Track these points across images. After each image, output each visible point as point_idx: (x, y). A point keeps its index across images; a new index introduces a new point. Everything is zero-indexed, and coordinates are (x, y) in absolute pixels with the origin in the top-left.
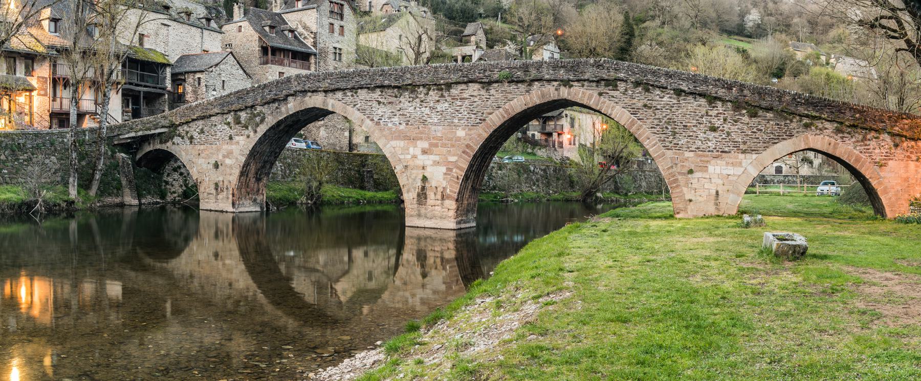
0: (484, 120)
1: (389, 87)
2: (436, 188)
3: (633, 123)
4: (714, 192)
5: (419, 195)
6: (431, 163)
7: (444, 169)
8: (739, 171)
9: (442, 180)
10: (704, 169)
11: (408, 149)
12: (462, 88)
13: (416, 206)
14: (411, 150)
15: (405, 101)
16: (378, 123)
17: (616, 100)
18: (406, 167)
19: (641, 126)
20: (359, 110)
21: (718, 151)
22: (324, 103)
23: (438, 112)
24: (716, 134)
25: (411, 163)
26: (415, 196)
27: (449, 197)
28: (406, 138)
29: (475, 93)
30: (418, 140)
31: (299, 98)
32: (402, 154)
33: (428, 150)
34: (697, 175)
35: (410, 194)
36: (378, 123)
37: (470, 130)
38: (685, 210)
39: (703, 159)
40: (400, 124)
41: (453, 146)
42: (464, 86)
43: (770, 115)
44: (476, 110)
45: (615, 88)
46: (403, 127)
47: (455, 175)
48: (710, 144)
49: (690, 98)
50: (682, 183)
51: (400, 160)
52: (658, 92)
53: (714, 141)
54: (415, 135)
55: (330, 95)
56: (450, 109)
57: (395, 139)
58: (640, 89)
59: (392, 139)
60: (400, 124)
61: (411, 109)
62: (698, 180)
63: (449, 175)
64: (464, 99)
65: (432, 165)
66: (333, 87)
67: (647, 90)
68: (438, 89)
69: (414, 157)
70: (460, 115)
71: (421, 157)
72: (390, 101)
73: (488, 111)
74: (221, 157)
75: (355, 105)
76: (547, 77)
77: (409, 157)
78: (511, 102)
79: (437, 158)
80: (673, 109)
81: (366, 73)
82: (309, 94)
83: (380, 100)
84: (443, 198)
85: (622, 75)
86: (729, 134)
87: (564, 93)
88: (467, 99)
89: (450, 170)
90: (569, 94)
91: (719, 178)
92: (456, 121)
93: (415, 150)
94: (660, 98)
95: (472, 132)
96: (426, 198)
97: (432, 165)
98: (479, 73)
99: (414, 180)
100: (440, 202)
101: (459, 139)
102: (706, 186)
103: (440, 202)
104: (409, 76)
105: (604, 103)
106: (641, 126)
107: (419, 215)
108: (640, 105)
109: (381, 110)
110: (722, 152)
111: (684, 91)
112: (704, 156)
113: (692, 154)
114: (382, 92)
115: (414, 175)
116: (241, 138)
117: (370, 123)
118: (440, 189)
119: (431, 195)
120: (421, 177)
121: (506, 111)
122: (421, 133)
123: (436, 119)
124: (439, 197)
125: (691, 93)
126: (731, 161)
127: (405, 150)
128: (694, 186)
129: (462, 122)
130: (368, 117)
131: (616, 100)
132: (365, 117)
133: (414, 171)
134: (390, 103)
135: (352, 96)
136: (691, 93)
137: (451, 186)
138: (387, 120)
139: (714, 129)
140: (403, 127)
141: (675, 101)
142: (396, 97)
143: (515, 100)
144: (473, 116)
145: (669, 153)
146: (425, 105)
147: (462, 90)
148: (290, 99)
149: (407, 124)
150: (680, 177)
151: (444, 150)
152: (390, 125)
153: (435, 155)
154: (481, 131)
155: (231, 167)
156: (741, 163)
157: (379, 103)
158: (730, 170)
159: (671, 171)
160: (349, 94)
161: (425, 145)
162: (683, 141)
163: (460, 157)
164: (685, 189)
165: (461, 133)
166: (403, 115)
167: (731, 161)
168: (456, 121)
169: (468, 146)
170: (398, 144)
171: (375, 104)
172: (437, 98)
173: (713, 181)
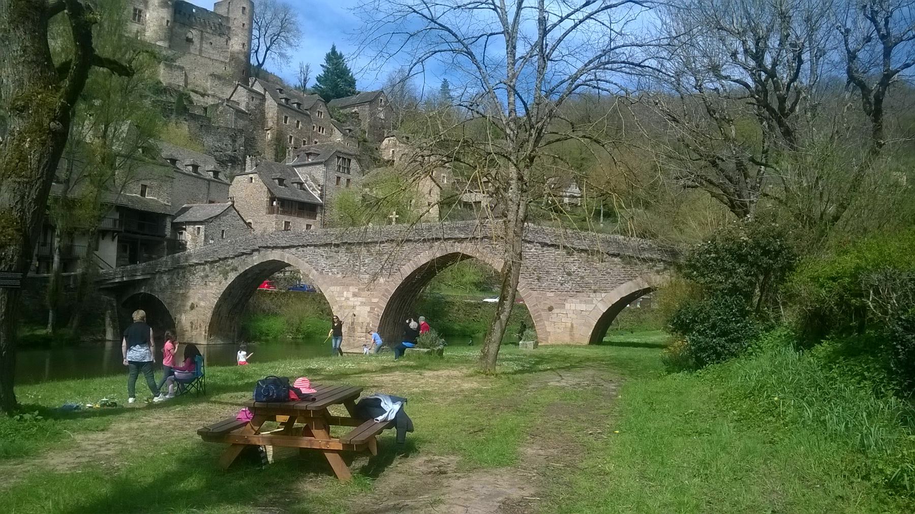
1: (330, 244)
7: (368, 309)
8: (590, 307)
10: (562, 306)
14: (345, 293)
16: (321, 273)
21: (573, 291)
25: (345, 304)
36: (321, 273)
38: (547, 339)
39: (561, 298)
40: (338, 273)
43: (616, 260)
46: (339, 276)
47: (376, 313)
53: (570, 284)
57: (333, 286)
60: (338, 273)
62: (557, 315)
63: (372, 313)
69: (347, 299)
71: (352, 299)
77: (343, 299)
79: (364, 300)
81: (314, 233)
91: (573, 313)
94: (529, 249)
102: (563, 320)
107: (349, 345)
113: (552, 294)
117: (316, 272)
121: (415, 263)
124: (364, 330)
125: (552, 245)
126: (584, 299)
127: (341, 294)
130: (314, 268)
132: (312, 267)
133: (347, 310)
152: (330, 274)
153: (363, 297)
158: (583, 307)
159: (535, 308)
163: (381, 299)
169: (387, 290)
173: (569, 316)
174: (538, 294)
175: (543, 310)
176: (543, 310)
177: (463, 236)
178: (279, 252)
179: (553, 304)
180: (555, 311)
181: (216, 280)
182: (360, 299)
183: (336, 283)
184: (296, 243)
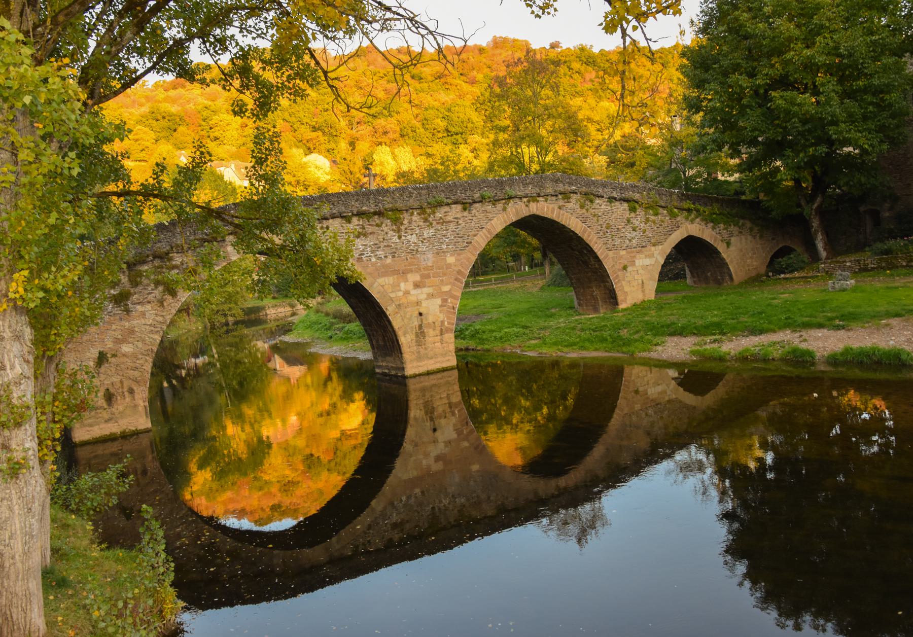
0: (471, 243)
2: (434, 323)
3: (585, 231)
4: (640, 282)
5: (417, 335)
6: (425, 296)
7: (438, 301)
9: (438, 314)
11: (399, 286)
12: (445, 210)
13: (415, 348)
14: (402, 285)
18: (399, 305)
19: (590, 233)
23: (424, 239)
25: (404, 301)
26: (413, 337)
28: (395, 272)
29: (458, 216)
30: (408, 273)
32: (392, 292)
33: (420, 282)
35: (408, 335)
37: (459, 255)
38: (625, 301)
40: (386, 257)
41: (445, 274)
44: (462, 233)
46: (389, 261)
47: (451, 305)
49: (617, 203)
51: (391, 299)
54: (404, 268)
59: (379, 276)
60: (386, 257)
63: (445, 306)
65: (426, 299)
69: (407, 293)
71: (413, 292)
73: (473, 233)
74: (110, 345)
77: (401, 294)
78: (492, 222)
84: (442, 333)
88: (451, 222)
89: (444, 301)
90: (537, 209)
92: (444, 247)
97: (426, 299)
98: (461, 193)
99: (410, 319)
100: (439, 337)
101: (449, 266)
103: (439, 337)
105: (563, 215)
106: (590, 233)
107: (419, 358)
110: (643, 247)
112: (632, 252)
115: (409, 314)
116: (149, 307)
118: (438, 324)
120: (417, 313)
121: (489, 231)
122: (410, 264)
123: (424, 247)
124: (438, 332)
127: (396, 287)
129: (450, 247)
136: (620, 200)
138: (370, 254)
140: (389, 261)
141: (609, 208)
143: (495, 219)
145: (611, 253)
146: (410, 232)
147: (446, 212)
149: (394, 257)
151: (437, 280)
152: (373, 260)
153: (429, 287)
154: (469, 255)
155: (134, 356)
156: (653, 254)
163: (453, 285)
164: (623, 282)
165: (451, 260)
166: (388, 246)
167: (647, 253)
168: (444, 247)
169: (459, 272)
170: (387, 281)
173: (639, 272)
174: (614, 253)
175: (619, 270)
176: (619, 270)
180: (629, 269)
181: (150, 297)
182: (426, 290)
183: (387, 271)
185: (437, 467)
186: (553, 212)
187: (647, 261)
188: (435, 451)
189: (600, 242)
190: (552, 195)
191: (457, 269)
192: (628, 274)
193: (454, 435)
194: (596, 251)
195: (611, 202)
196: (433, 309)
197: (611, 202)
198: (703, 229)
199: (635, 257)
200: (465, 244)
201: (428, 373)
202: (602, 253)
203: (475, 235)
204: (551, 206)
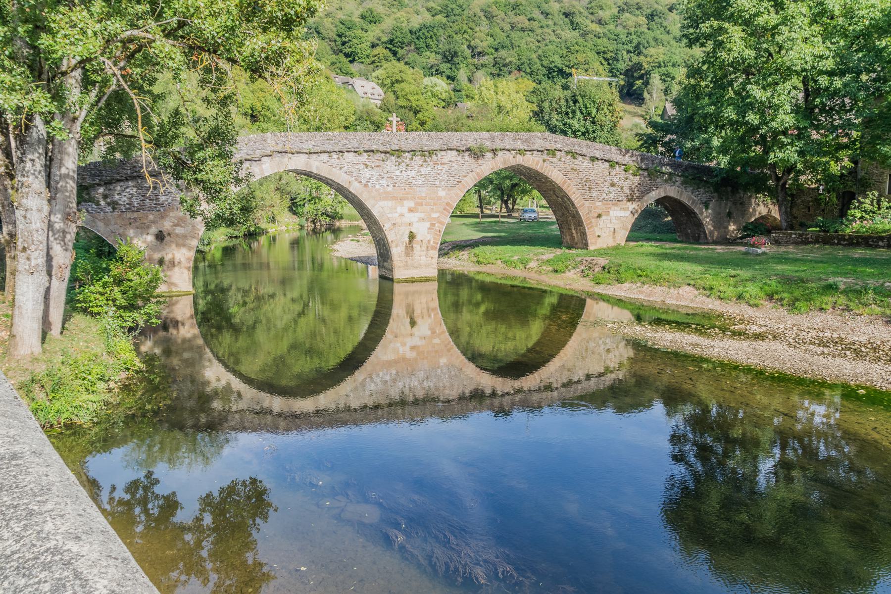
3: (565, 182)
5: (406, 247)
6: (417, 219)
7: (428, 225)
13: (404, 258)
14: (399, 209)
15: (390, 164)
16: (366, 186)
17: (555, 165)
20: (346, 173)
22: (307, 164)
24: (614, 189)
26: (403, 249)
27: (433, 248)
28: (394, 198)
31: (277, 158)
34: (603, 218)
35: (399, 248)
38: (595, 243)
41: (435, 204)
42: (443, 153)
43: (646, 173)
45: (554, 155)
48: (611, 195)
50: (594, 224)
52: (580, 158)
55: (315, 156)
56: (432, 173)
58: (569, 156)
61: (398, 173)
64: (444, 164)
66: (318, 149)
67: (575, 158)
68: (422, 155)
69: (402, 215)
70: (441, 178)
72: (377, 164)
73: (464, 174)
75: (341, 168)
76: (508, 147)
77: (397, 215)
79: (422, 215)
80: (590, 171)
82: (290, 155)
83: (367, 163)
85: (559, 146)
86: (622, 188)
87: (520, 160)
90: (523, 161)
92: (437, 183)
93: (403, 209)
95: (452, 192)
96: (412, 250)
99: (402, 235)
101: (440, 198)
104: (396, 142)
105: (546, 167)
107: (406, 266)
108: (569, 168)
109: (367, 173)
111: (597, 159)
112: (607, 204)
114: (369, 156)
117: (358, 185)
118: (425, 242)
119: (416, 247)
120: (408, 232)
121: (478, 174)
124: (424, 248)
128: (601, 226)
130: (356, 180)
131: (555, 165)
134: (377, 166)
135: (338, 158)
137: (434, 238)
139: (613, 185)
140: (390, 188)
142: (383, 161)
144: (451, 178)
145: (587, 203)
148: (265, 159)
150: (593, 220)
154: (459, 192)
157: (367, 166)
160: (334, 156)
161: (411, 204)
162: (594, 194)
163: (442, 213)
165: (442, 193)
166: (391, 177)
167: (623, 207)
168: (437, 183)
169: (448, 204)
171: (362, 167)
172: (421, 163)
174: (590, 203)
175: (593, 217)
176: (593, 217)
177: (526, 148)
178: (303, 157)
179: (600, 212)
183: (387, 196)
184: (329, 147)
185: (411, 355)
186: (537, 164)
187: (622, 214)
188: (410, 342)
189: (578, 193)
190: (538, 151)
191: (446, 201)
192: (601, 222)
193: (429, 333)
194: (573, 200)
195: (593, 161)
196: (423, 231)
197: (593, 161)
198: (682, 192)
199: (610, 208)
200: (456, 182)
201: (413, 281)
202: (578, 203)
203: (465, 176)
204: (536, 159)
